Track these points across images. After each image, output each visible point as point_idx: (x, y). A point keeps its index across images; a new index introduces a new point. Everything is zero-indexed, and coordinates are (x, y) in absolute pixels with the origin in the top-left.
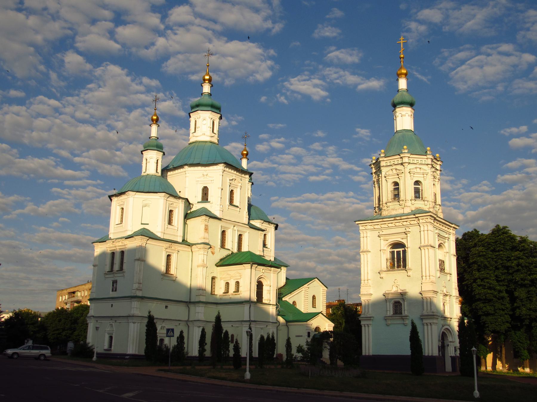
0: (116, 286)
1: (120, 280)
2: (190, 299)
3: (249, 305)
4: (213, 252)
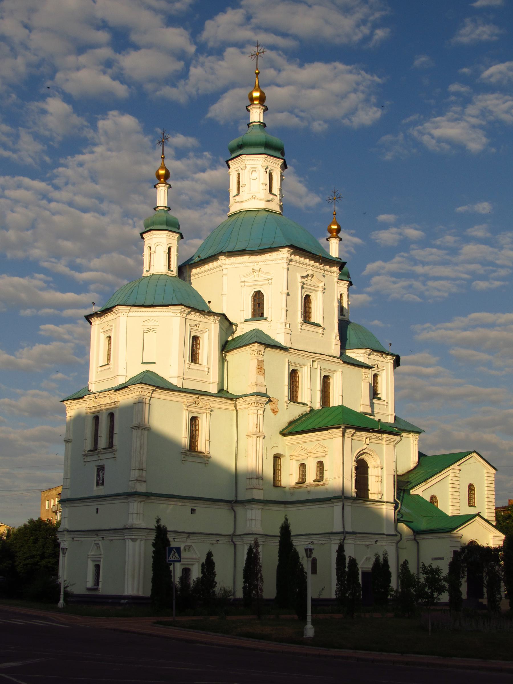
0: (103, 476)
1: (109, 465)
2: (236, 496)
3: (342, 503)
4: (275, 410)
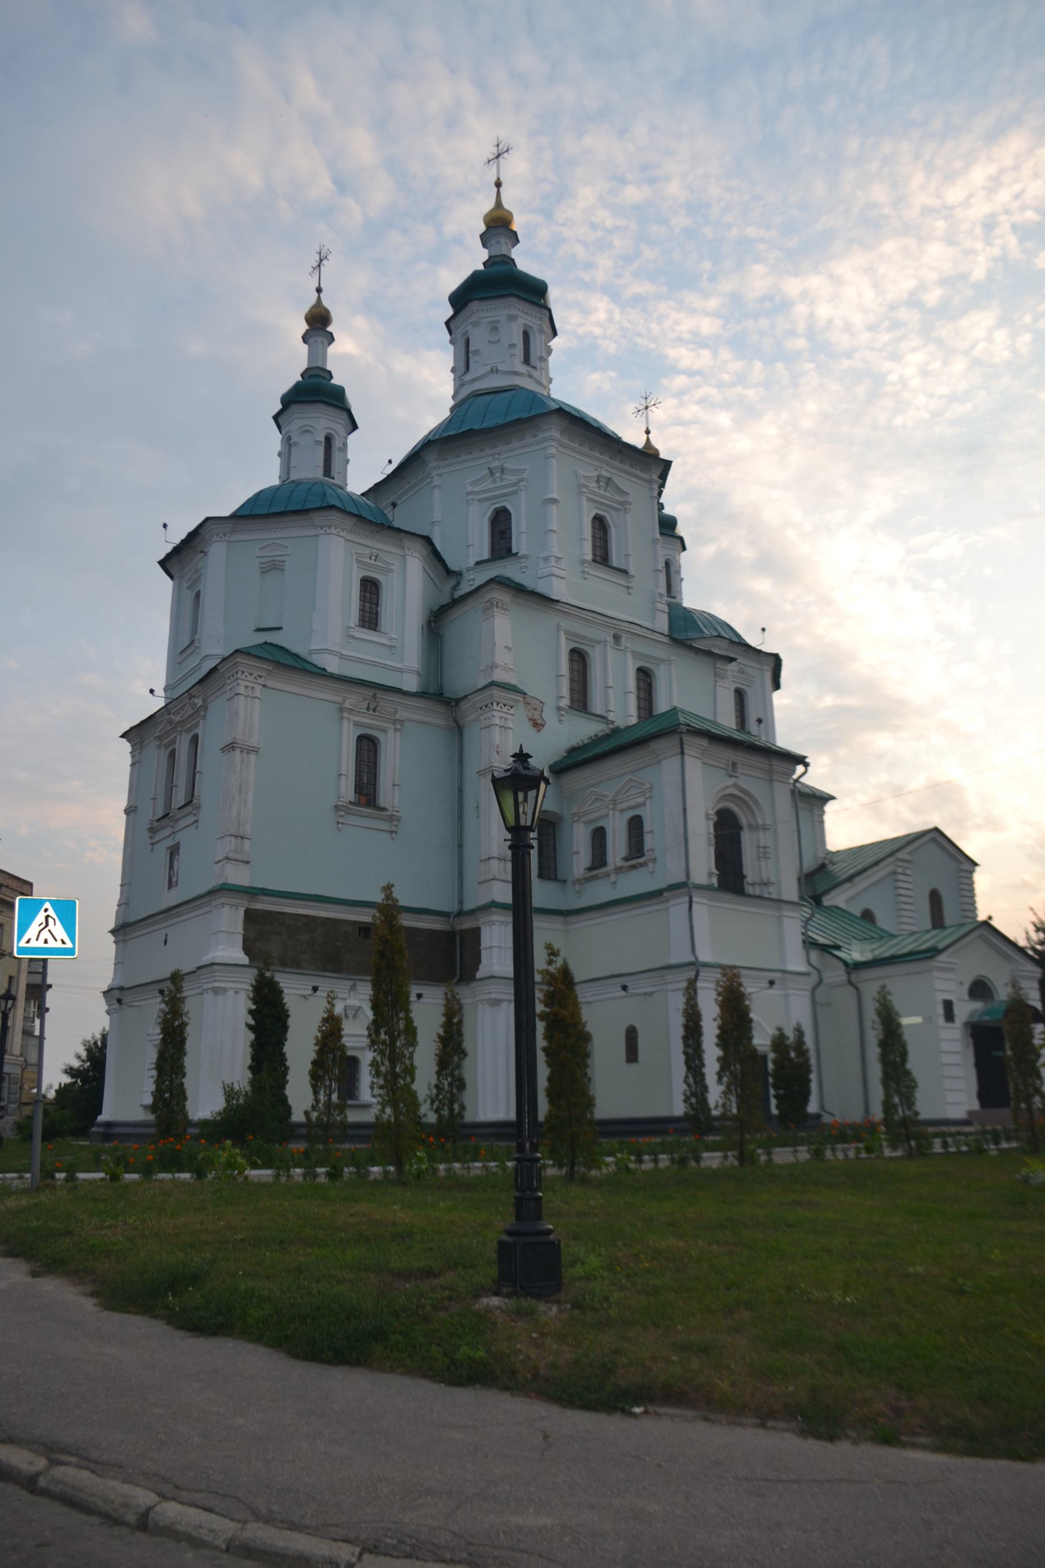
2: (461, 902)
3: (687, 899)
4: (539, 722)
